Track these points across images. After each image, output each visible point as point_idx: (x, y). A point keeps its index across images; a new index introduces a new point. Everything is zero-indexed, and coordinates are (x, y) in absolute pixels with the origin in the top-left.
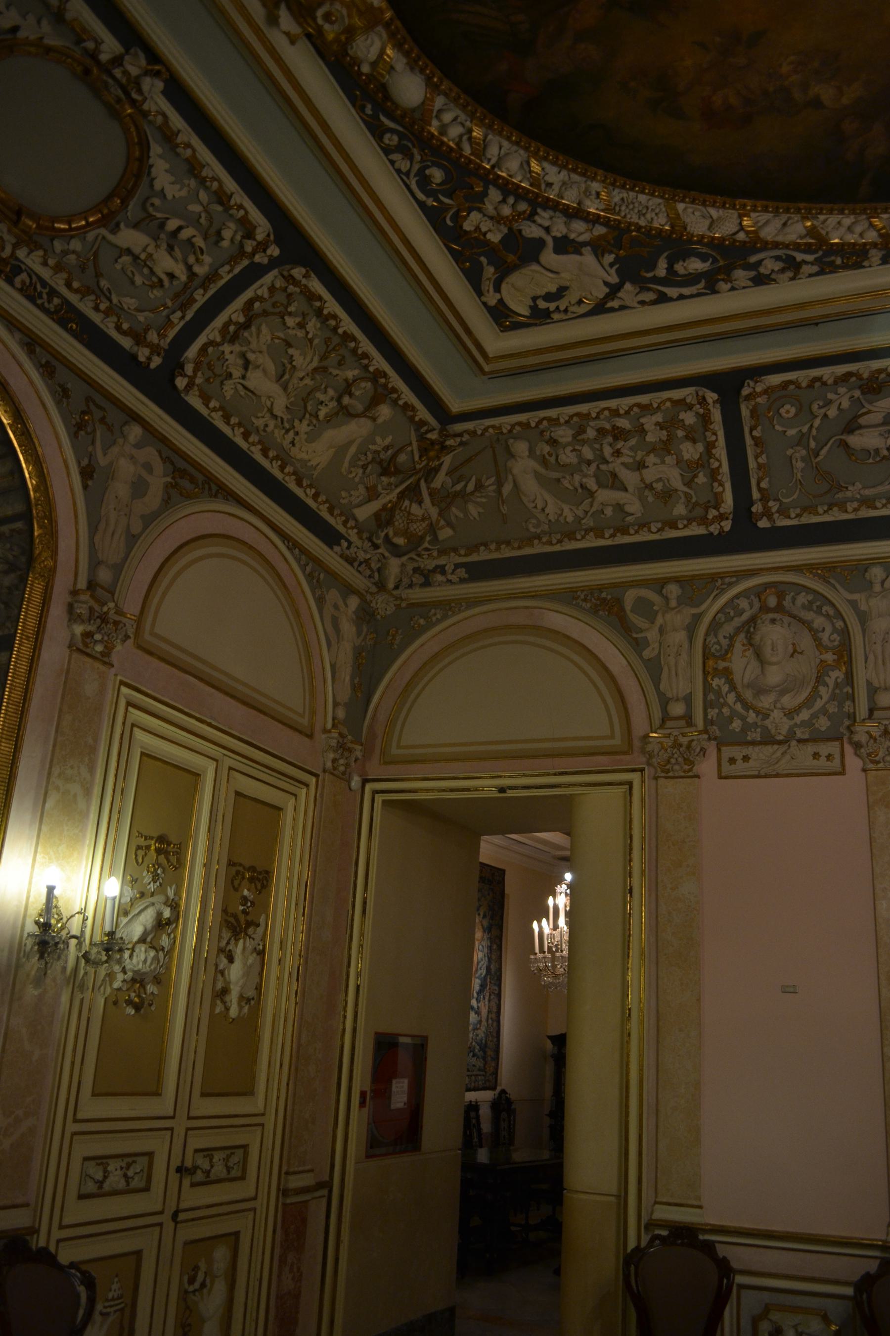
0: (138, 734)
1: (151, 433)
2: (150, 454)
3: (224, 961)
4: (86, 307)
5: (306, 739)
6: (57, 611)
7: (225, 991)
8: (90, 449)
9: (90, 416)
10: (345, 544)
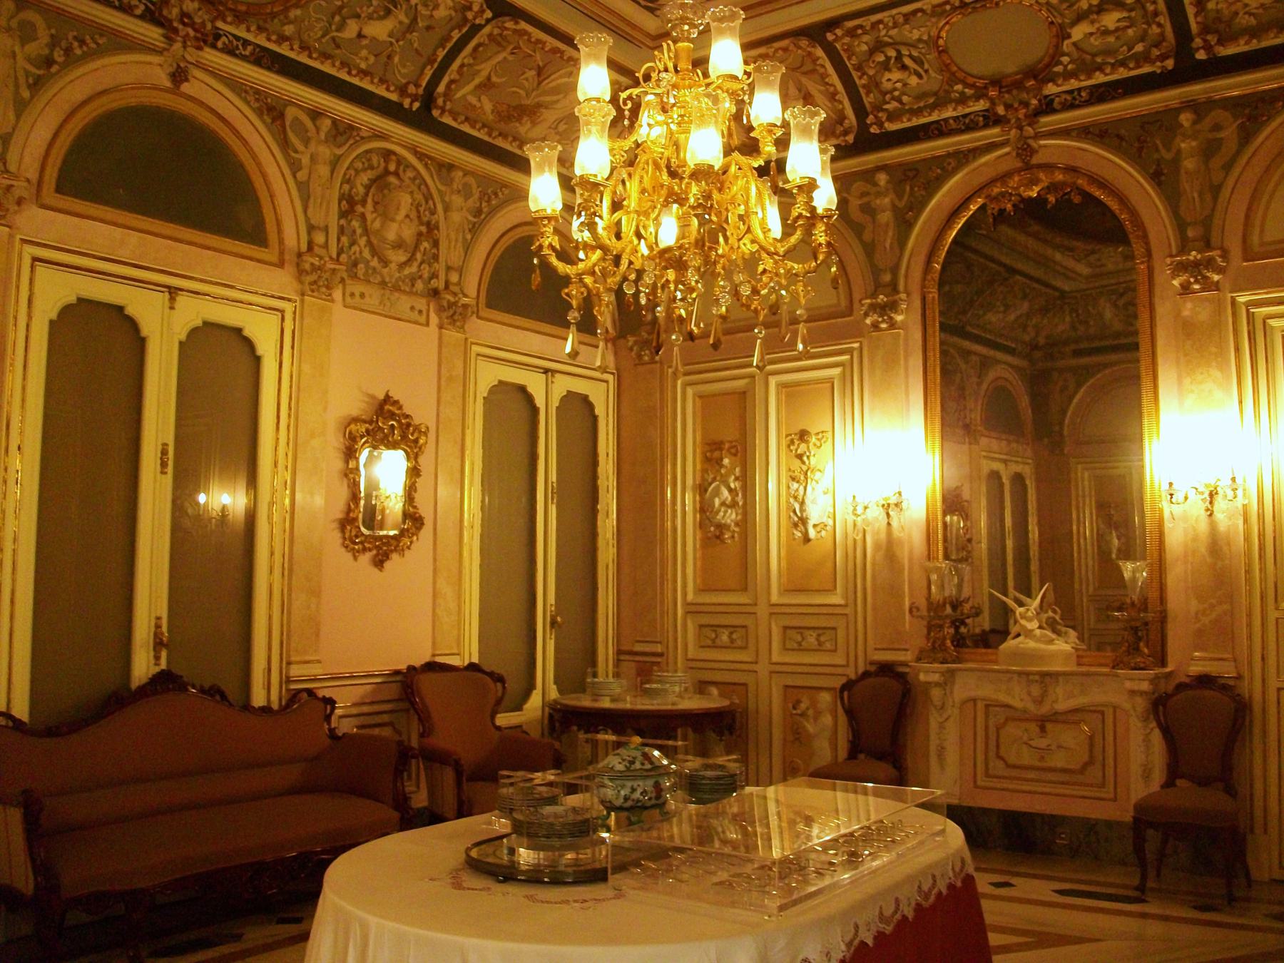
2: (1219, 115)
4: (1099, 78)
8: (1156, 156)
9: (1134, 140)
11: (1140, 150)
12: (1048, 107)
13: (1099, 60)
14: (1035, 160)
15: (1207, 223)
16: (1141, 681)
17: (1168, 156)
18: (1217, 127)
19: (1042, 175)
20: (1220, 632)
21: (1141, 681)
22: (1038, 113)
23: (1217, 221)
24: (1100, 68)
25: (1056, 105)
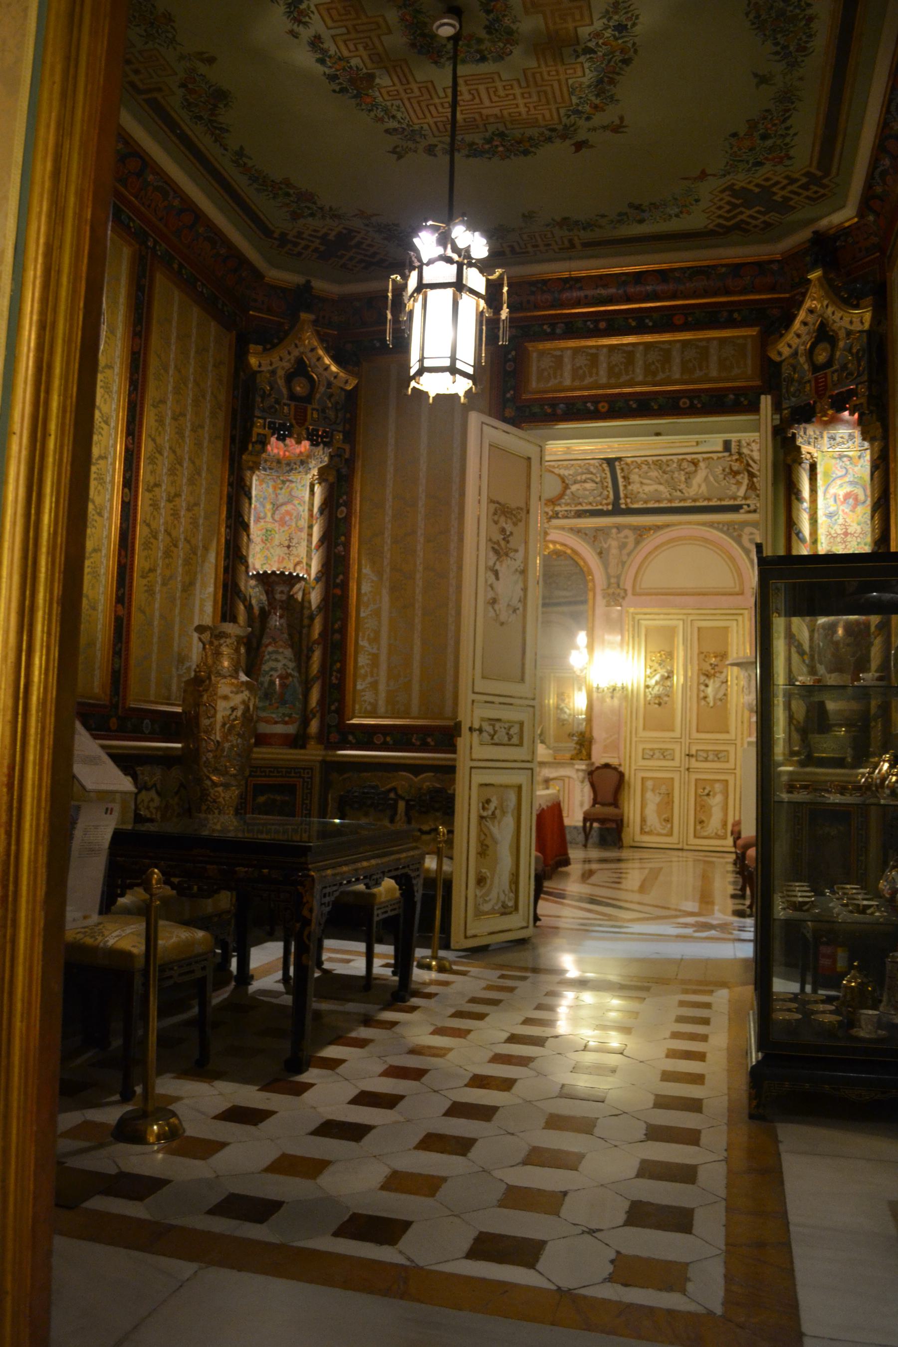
0: (642, 622)
1: (619, 528)
2: (627, 532)
3: (702, 687)
4: (580, 508)
5: (740, 597)
6: (599, 597)
7: (705, 698)
10: (745, 507)
11: (594, 541)
12: (556, 516)
13: (581, 500)
14: (549, 538)
15: (618, 577)
16: (583, 766)
17: (605, 546)
18: (626, 537)
19: (551, 546)
20: (614, 746)
21: (583, 766)
22: (551, 518)
23: (623, 578)
24: (580, 504)
25: (560, 516)
